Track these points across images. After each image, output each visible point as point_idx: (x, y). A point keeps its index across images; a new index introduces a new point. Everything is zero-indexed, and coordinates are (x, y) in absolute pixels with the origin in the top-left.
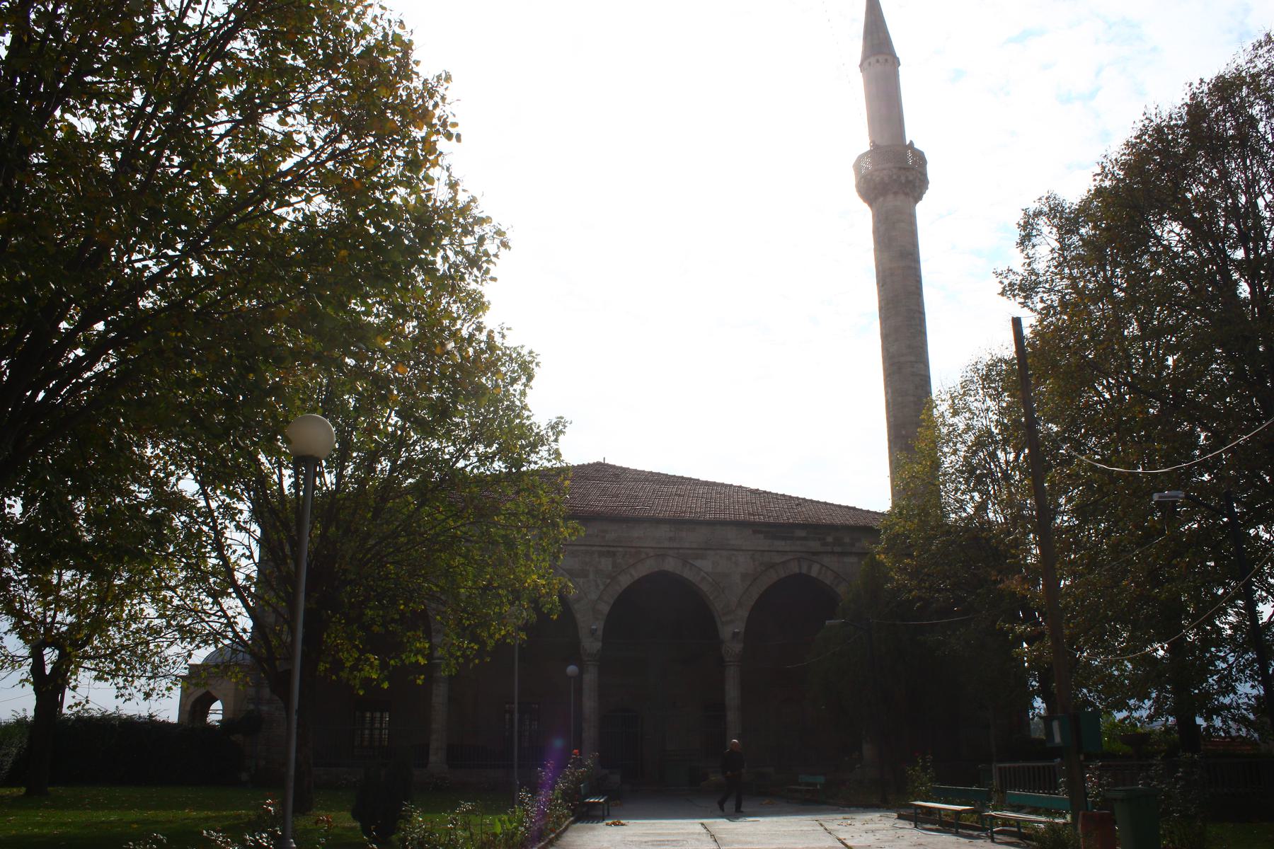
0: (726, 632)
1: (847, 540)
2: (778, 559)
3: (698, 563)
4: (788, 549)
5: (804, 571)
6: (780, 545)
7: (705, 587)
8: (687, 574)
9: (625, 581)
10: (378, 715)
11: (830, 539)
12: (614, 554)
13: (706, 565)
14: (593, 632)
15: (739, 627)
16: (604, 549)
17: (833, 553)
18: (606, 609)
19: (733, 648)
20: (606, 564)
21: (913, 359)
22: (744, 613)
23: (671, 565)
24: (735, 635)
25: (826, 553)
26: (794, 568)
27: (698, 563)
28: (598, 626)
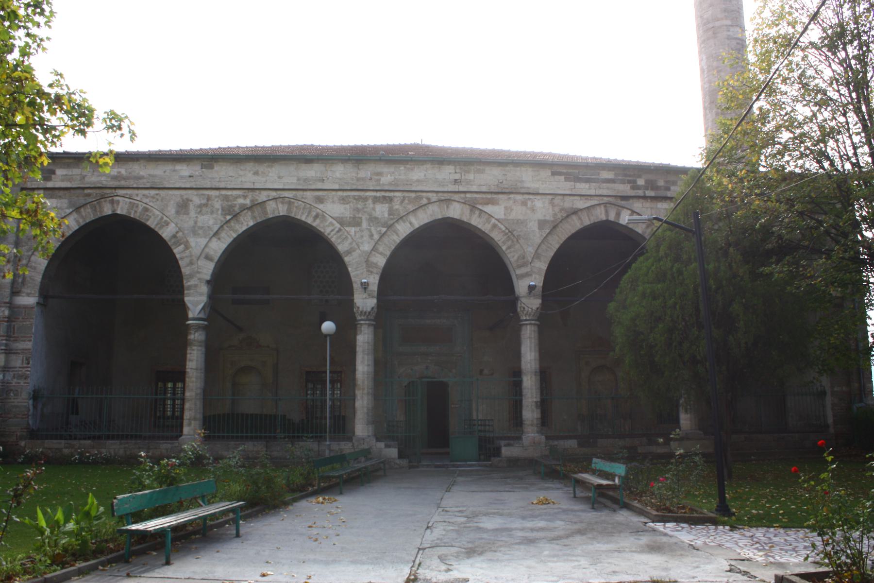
0: (521, 287)
1: (661, 183)
2: (581, 204)
3: (489, 209)
4: (592, 192)
5: (612, 217)
6: (583, 188)
7: (497, 237)
8: (476, 221)
9: (404, 230)
10: (170, 385)
11: (641, 182)
12: (390, 200)
13: (497, 211)
14: (365, 286)
15: (537, 280)
16: (378, 194)
17: (645, 198)
18: (381, 261)
19: (530, 304)
20: (381, 210)
21: (728, 22)
22: (542, 266)
23: (456, 211)
24: (531, 288)
25: (639, 197)
26: (600, 215)
27: (489, 209)
28: (374, 281)
